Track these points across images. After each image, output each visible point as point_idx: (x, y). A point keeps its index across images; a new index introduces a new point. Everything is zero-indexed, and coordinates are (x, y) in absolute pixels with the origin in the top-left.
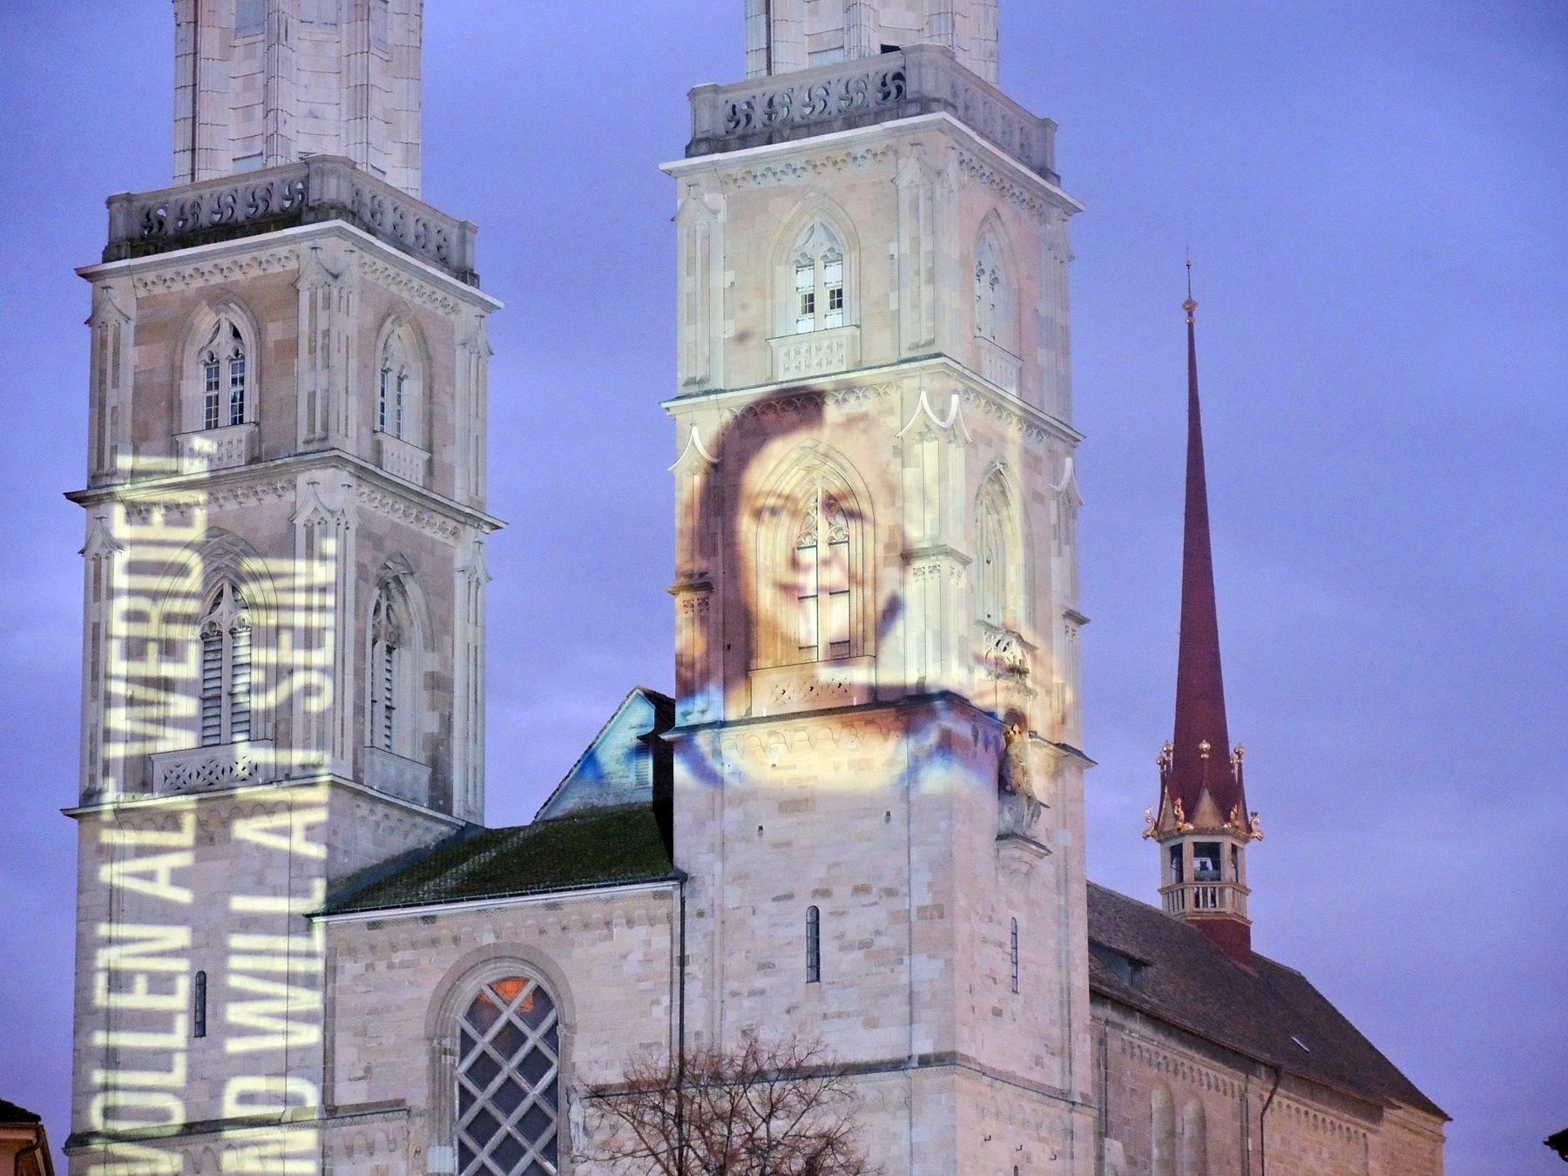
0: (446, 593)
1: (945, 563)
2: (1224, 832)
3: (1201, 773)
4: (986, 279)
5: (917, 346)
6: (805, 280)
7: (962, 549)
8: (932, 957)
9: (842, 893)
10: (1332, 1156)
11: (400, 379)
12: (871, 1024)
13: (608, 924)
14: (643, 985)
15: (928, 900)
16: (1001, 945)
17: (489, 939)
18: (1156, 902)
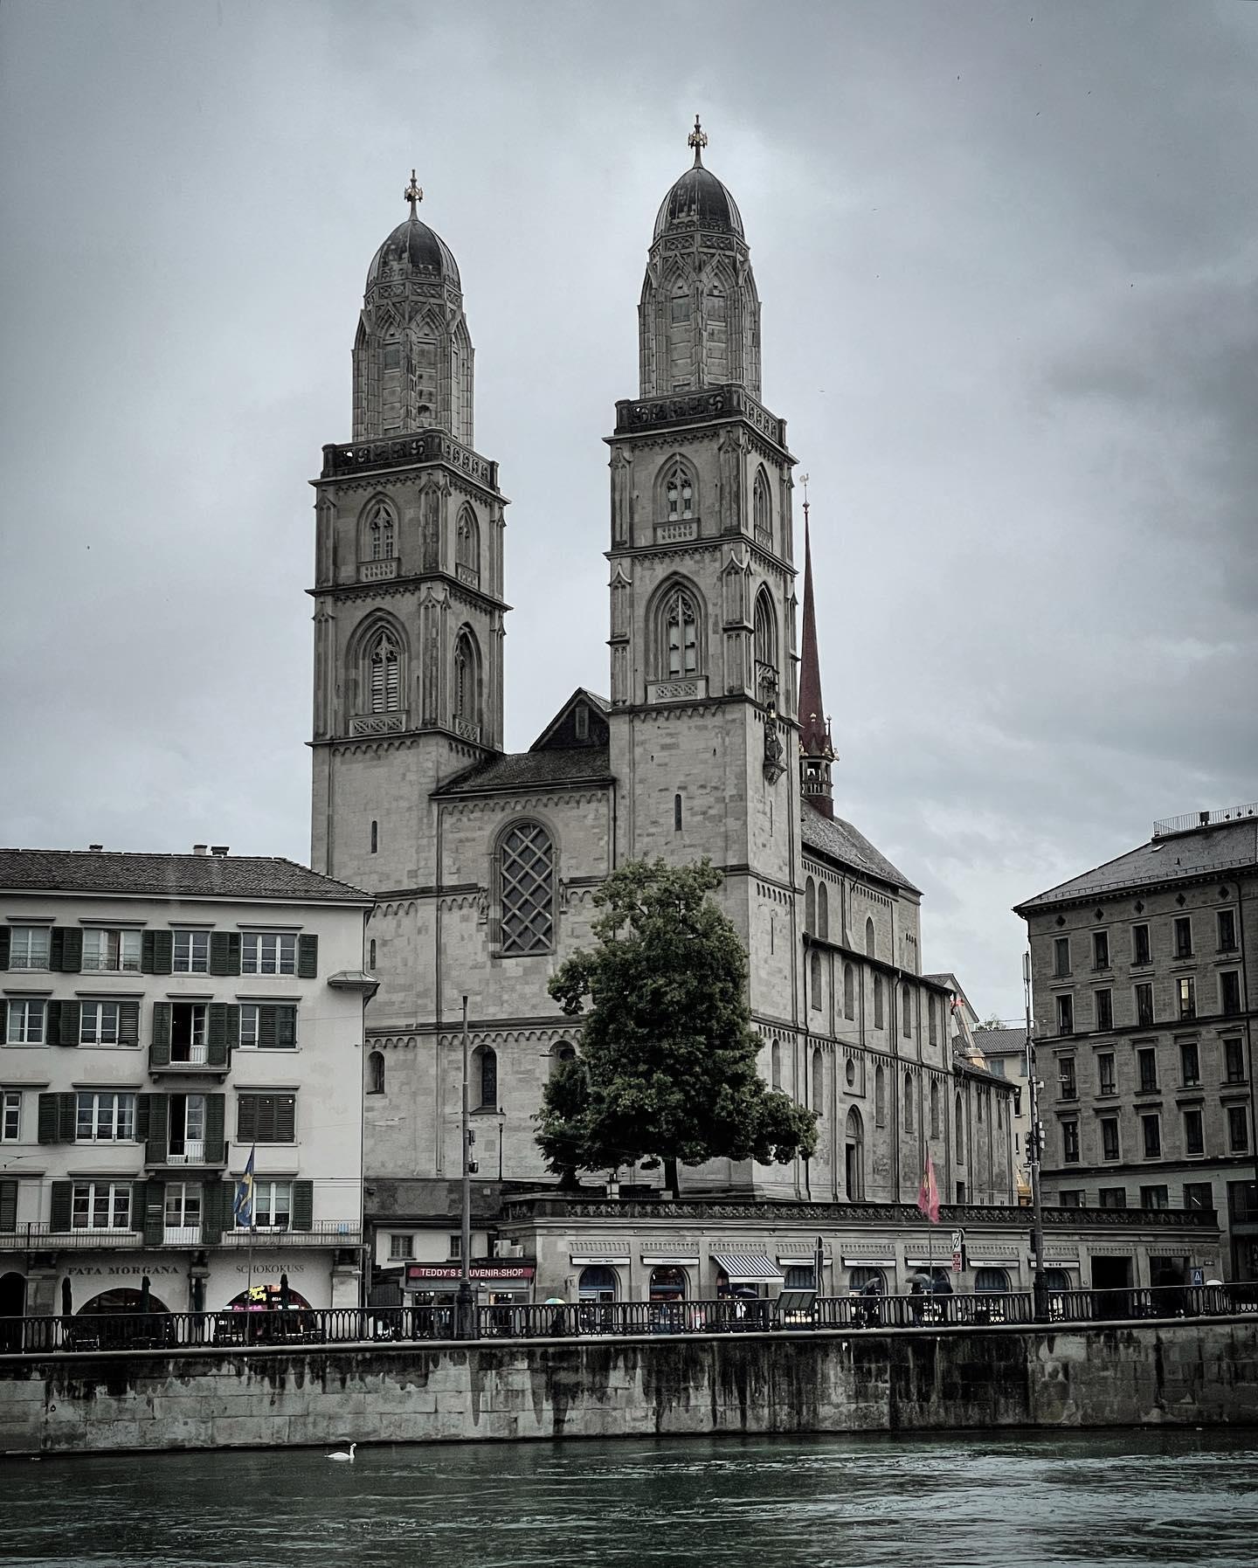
6: (673, 495)
9: (693, 789)
15: (734, 792)
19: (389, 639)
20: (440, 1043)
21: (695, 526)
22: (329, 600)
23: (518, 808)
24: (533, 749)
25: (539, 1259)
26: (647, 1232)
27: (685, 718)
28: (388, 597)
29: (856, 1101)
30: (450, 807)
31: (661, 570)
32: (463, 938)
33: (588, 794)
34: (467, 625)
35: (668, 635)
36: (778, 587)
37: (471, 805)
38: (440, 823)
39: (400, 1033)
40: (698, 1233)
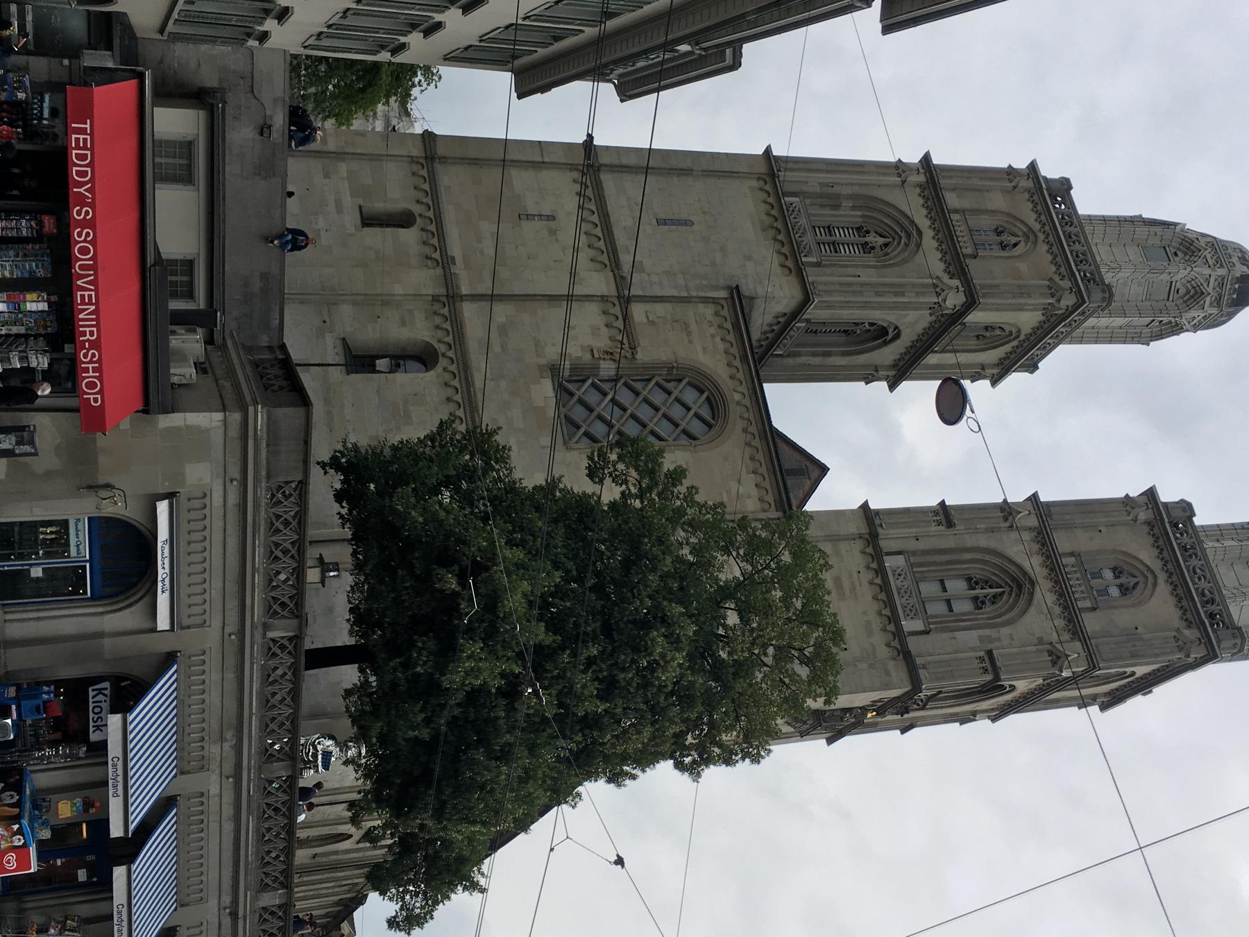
6: (1108, 574)
11: (978, 337)
13: (754, 472)
19: (886, 245)
20: (435, 299)
22: (921, 178)
23: (737, 397)
25: (166, 421)
26: (231, 661)
27: (876, 606)
28: (935, 244)
30: (725, 312)
31: (1034, 565)
33: (767, 484)
34: (897, 336)
35: (958, 577)
37: (731, 337)
38: (705, 300)
39: (443, 248)
40: (229, 768)
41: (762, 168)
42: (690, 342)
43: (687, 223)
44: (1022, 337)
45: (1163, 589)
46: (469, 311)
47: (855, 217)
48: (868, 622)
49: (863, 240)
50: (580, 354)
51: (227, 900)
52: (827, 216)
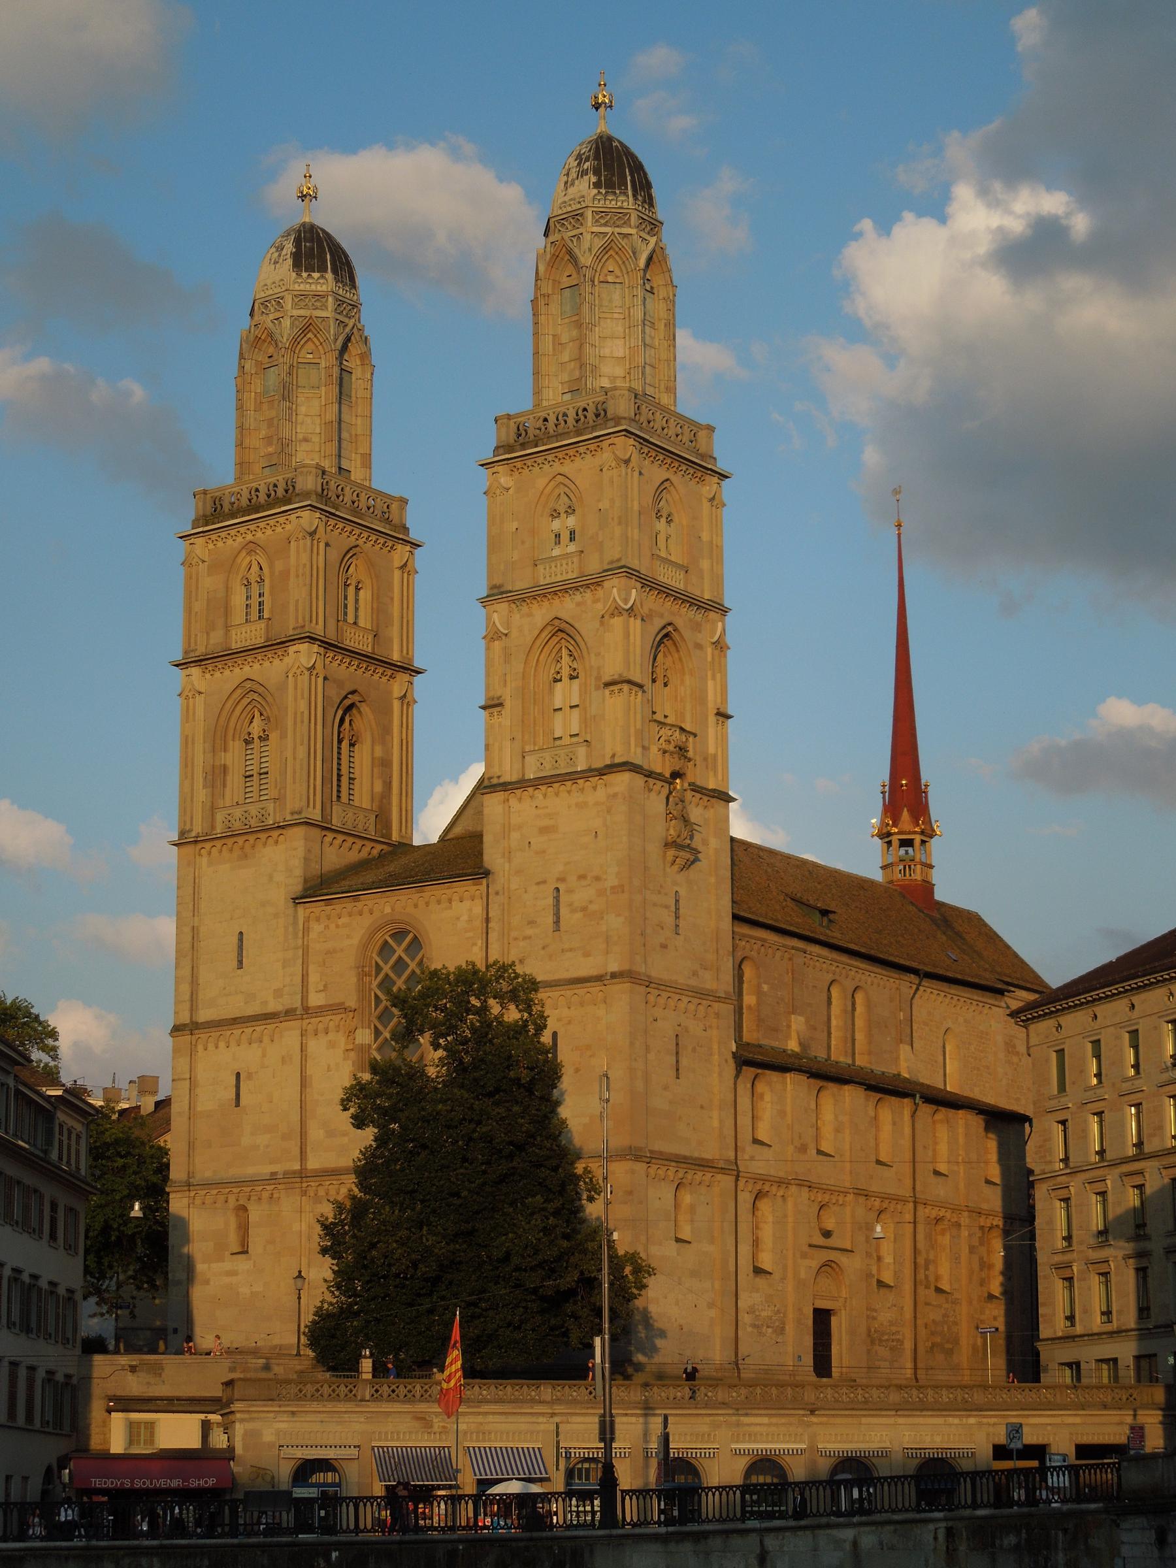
0: (388, 711)
1: (626, 687)
2: (915, 833)
3: (906, 797)
4: (663, 520)
5: (612, 562)
6: (556, 525)
7: (637, 678)
8: (619, 915)
10: (965, 1021)
11: (357, 589)
12: (587, 955)
13: (450, 901)
14: (470, 934)
15: (616, 882)
16: (667, 907)
17: (388, 910)
18: (877, 876)
21: (575, 560)
23: (388, 910)
24: (442, 839)
25: (239, 1450)
28: (256, 666)
29: (833, 1256)
32: (329, 1069)
35: (551, 691)
36: (697, 627)
38: (306, 930)
41: (189, 849)
42: (342, 950)
43: (241, 933)
44: (360, 542)
45: (568, 468)
46: (313, 1164)
47: (236, 747)
48: (577, 805)
49: (256, 740)
50: (350, 1062)
51: (541, 1419)
52: (235, 780)
